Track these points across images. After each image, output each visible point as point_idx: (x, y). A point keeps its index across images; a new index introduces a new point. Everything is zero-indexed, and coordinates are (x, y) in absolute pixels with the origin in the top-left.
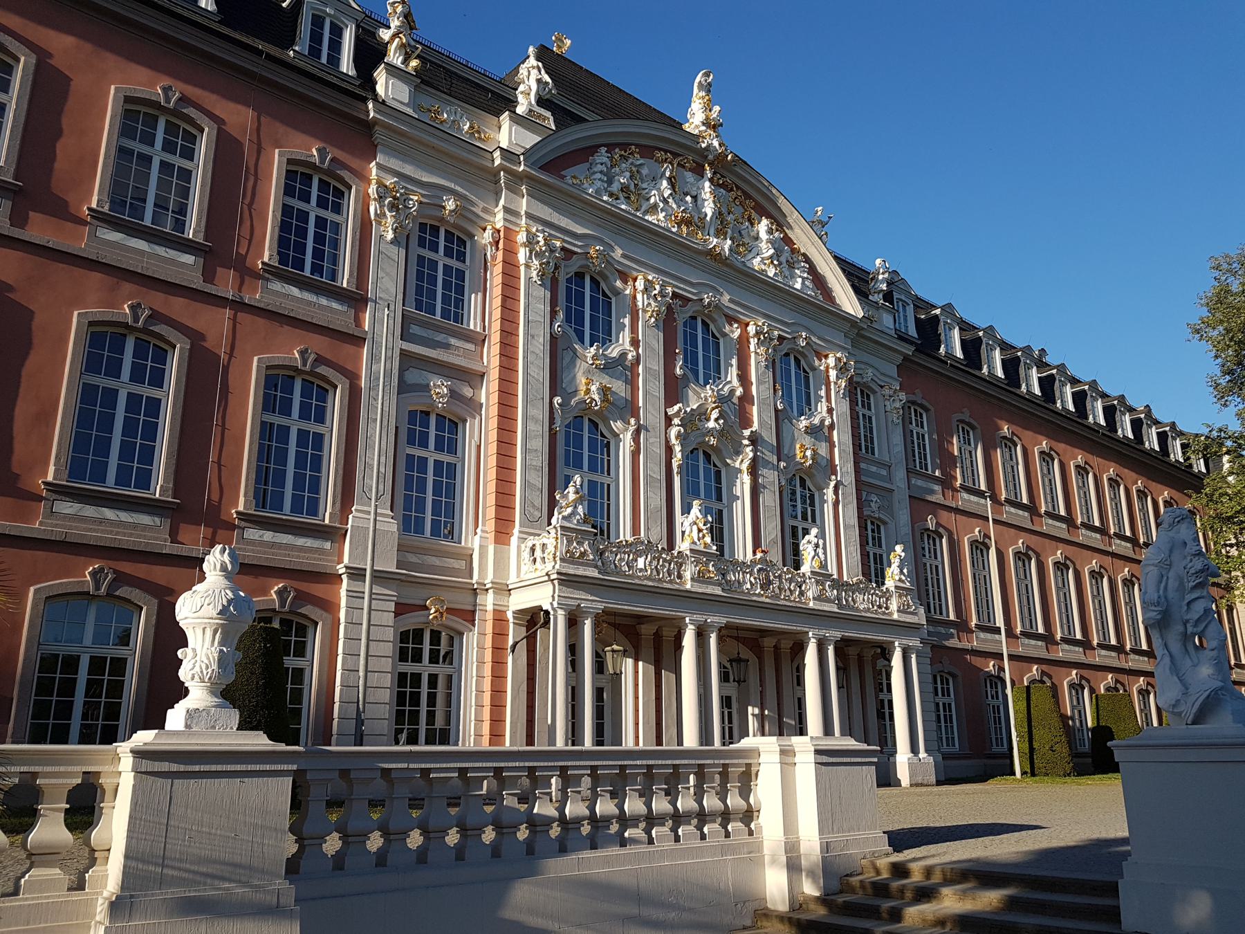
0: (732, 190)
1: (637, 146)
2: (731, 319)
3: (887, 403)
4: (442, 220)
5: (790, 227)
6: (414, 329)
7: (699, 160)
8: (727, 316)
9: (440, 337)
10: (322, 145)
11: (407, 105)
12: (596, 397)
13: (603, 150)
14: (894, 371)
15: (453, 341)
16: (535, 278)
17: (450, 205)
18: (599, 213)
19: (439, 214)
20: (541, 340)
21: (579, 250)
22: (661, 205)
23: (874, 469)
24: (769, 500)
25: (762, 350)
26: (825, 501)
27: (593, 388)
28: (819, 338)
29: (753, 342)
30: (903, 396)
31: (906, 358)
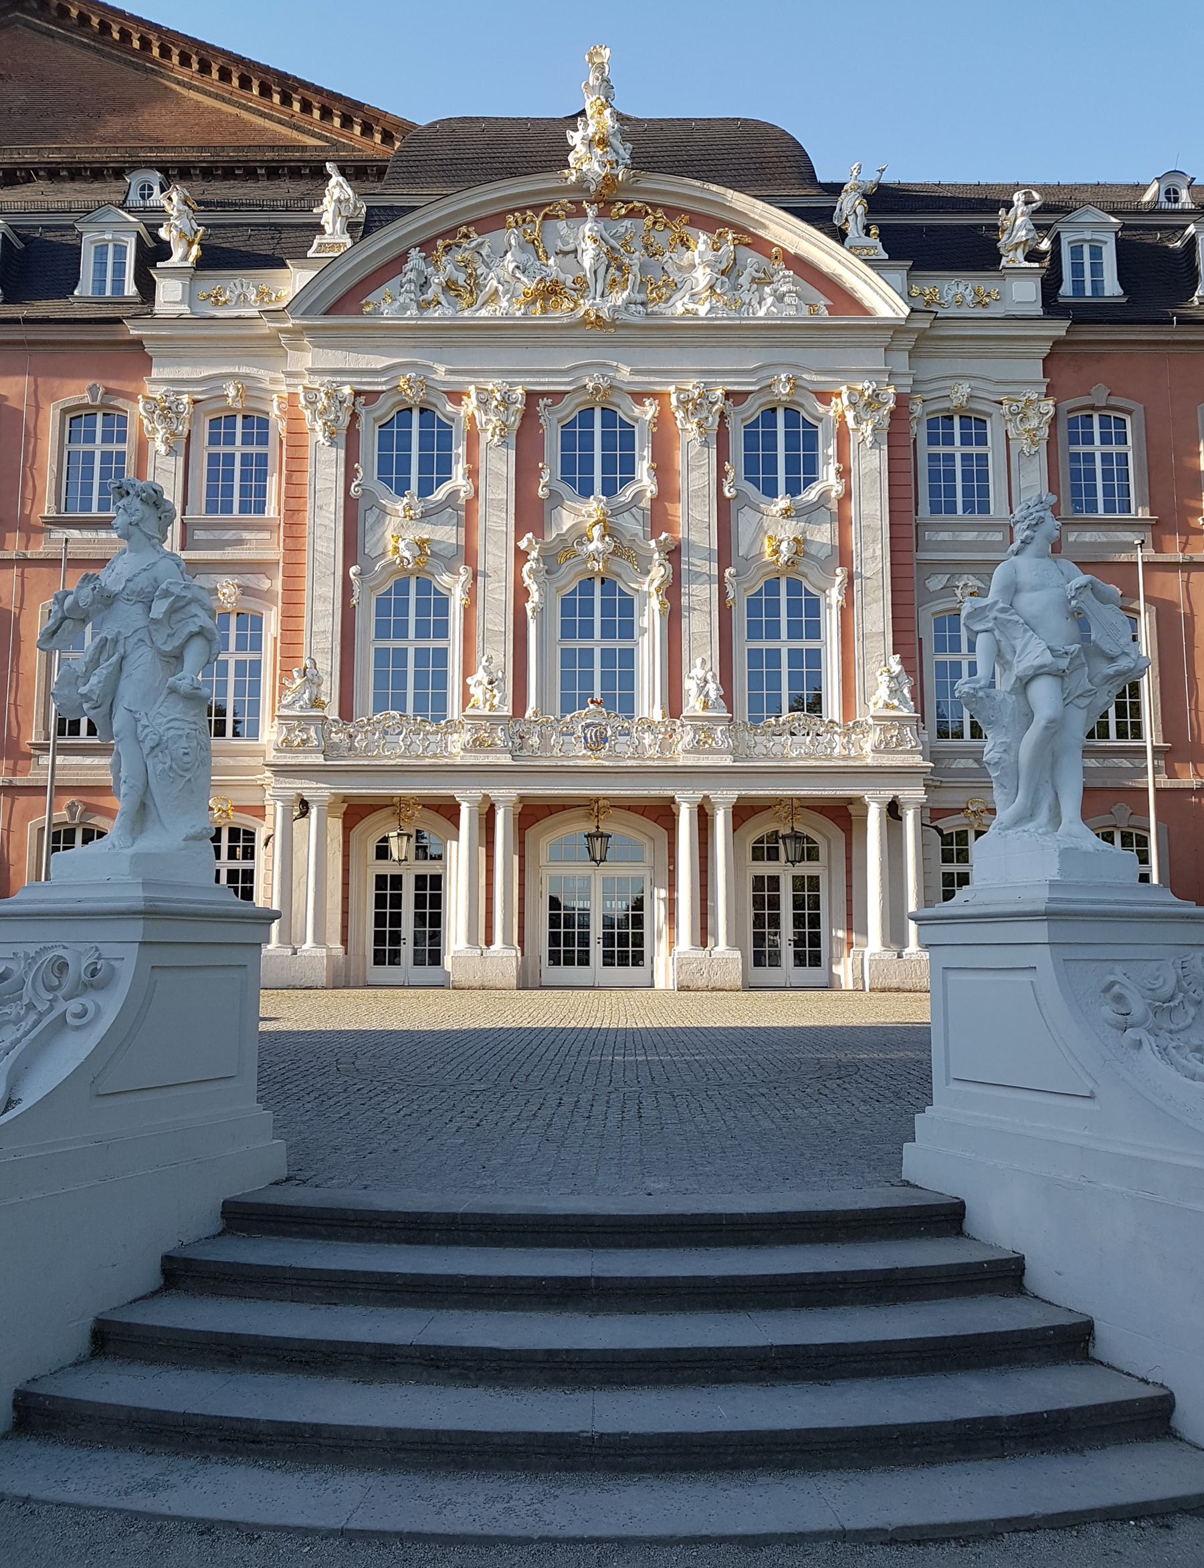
0: (647, 214)
1: (468, 224)
2: (638, 397)
3: (1010, 426)
4: (230, 408)
5: (764, 226)
6: (199, 535)
7: (576, 197)
8: (632, 394)
9: (229, 535)
10: (90, 383)
11: (181, 302)
12: (407, 554)
13: (414, 253)
14: (1035, 369)
15: (246, 535)
16: (322, 440)
17: (232, 392)
18: (409, 333)
19: (221, 404)
20: (332, 508)
21: (384, 388)
22: (500, 288)
23: (970, 536)
24: (701, 626)
25: (692, 426)
26: (830, 606)
27: (402, 545)
28: (819, 372)
29: (680, 415)
30: (1048, 406)
31: (1058, 342)
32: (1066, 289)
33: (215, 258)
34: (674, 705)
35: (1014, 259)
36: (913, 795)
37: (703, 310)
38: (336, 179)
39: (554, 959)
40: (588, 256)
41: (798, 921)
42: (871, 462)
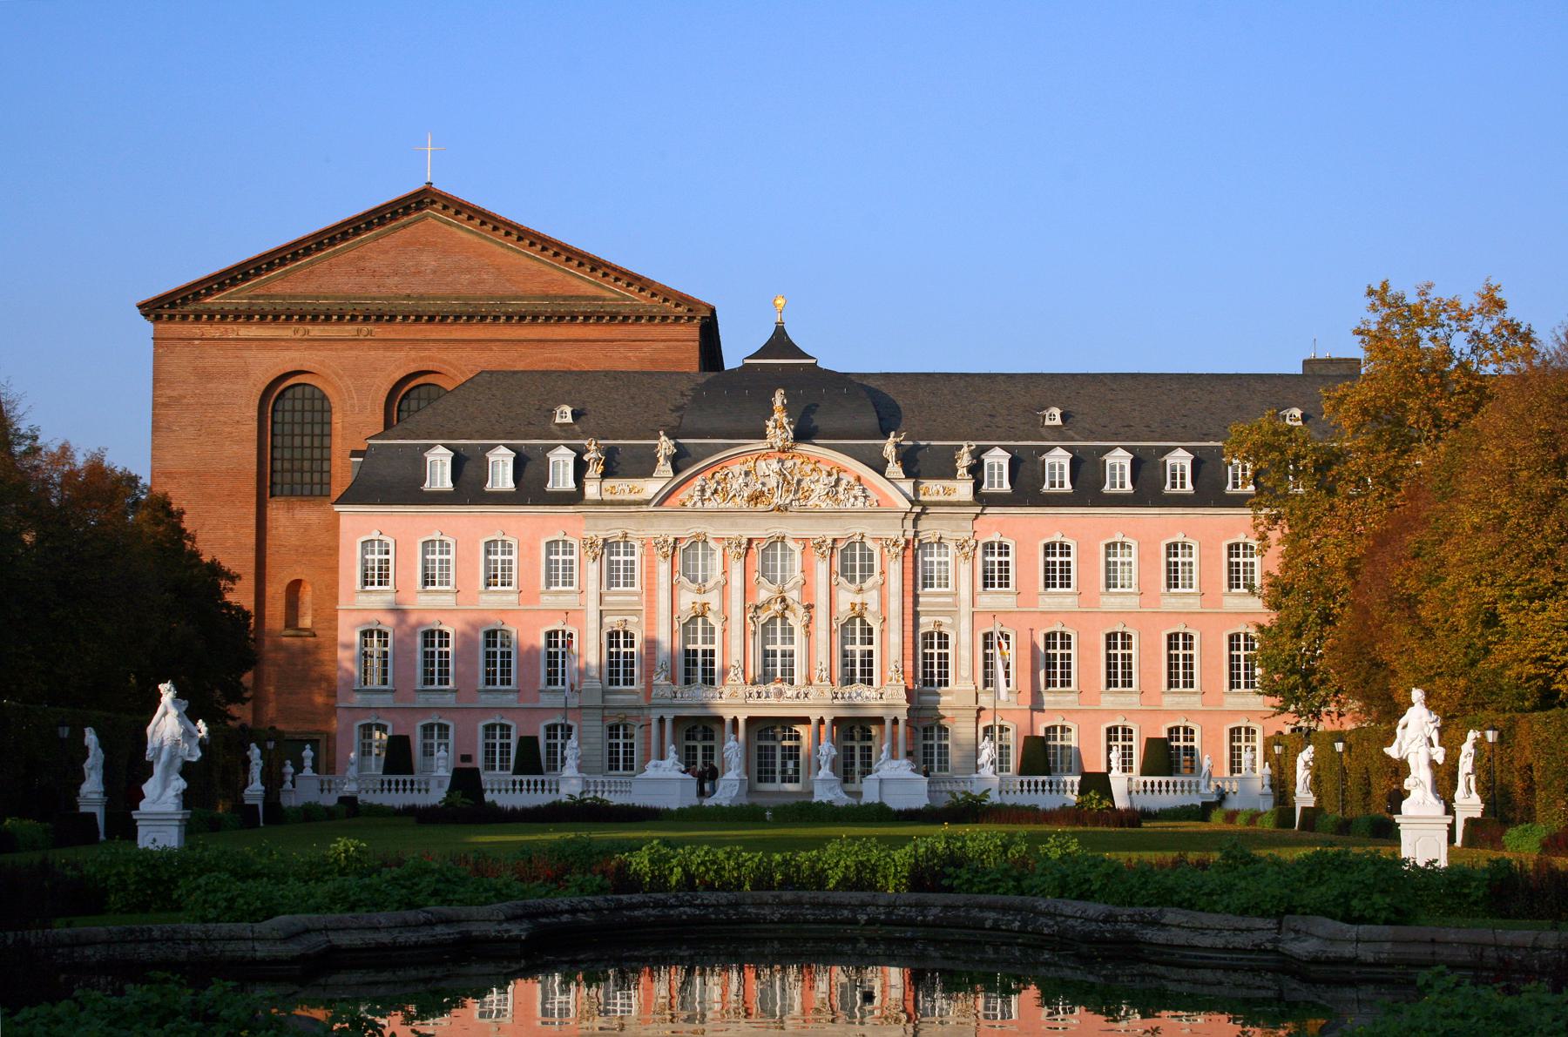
32: (985, 486)
33: (610, 471)
34: (809, 682)
35: (962, 471)
36: (903, 716)
37: (823, 505)
38: (663, 438)
39: (760, 780)
40: (772, 482)
41: (862, 764)
42: (894, 569)
